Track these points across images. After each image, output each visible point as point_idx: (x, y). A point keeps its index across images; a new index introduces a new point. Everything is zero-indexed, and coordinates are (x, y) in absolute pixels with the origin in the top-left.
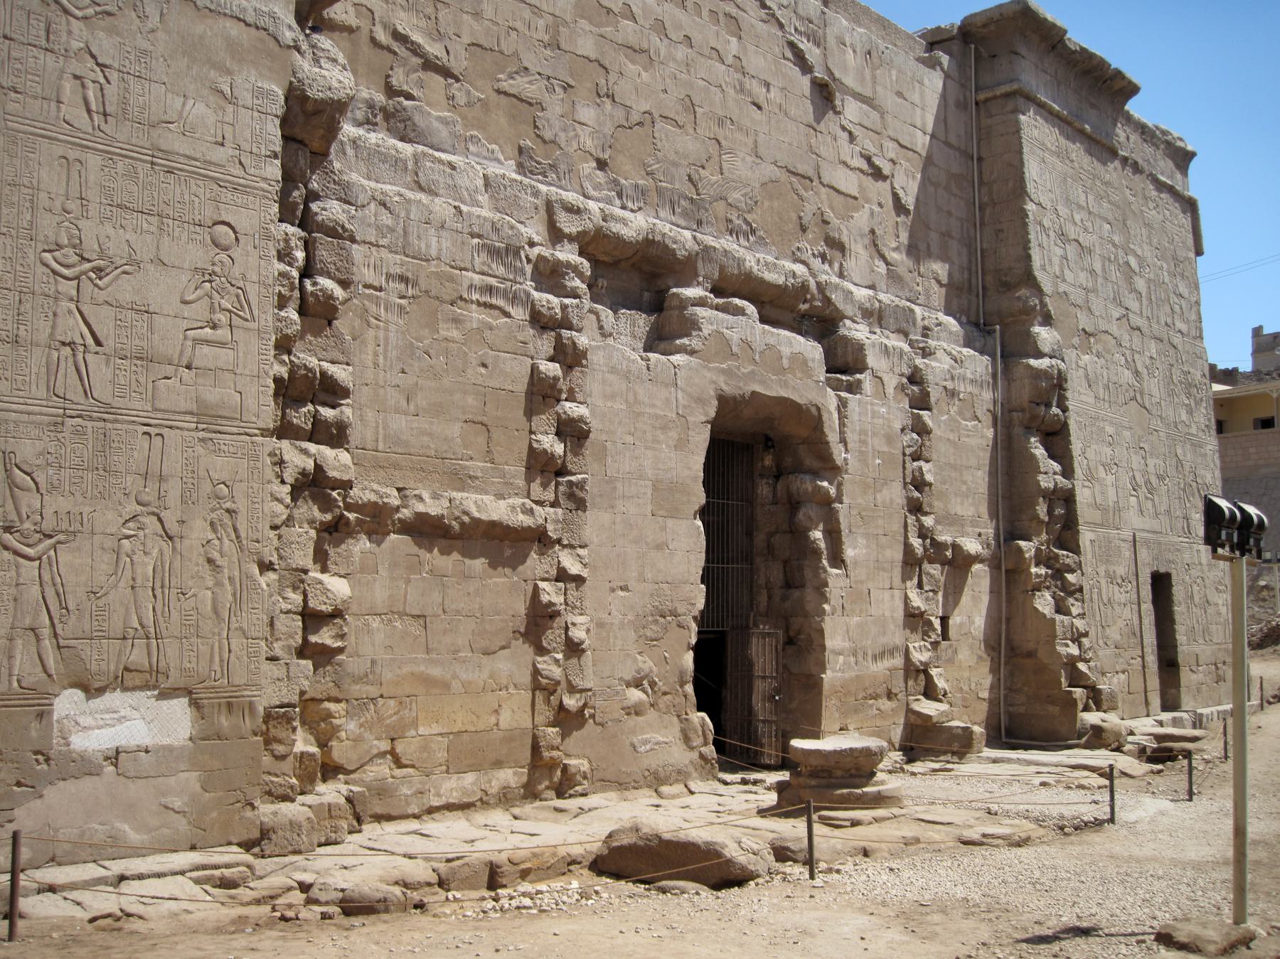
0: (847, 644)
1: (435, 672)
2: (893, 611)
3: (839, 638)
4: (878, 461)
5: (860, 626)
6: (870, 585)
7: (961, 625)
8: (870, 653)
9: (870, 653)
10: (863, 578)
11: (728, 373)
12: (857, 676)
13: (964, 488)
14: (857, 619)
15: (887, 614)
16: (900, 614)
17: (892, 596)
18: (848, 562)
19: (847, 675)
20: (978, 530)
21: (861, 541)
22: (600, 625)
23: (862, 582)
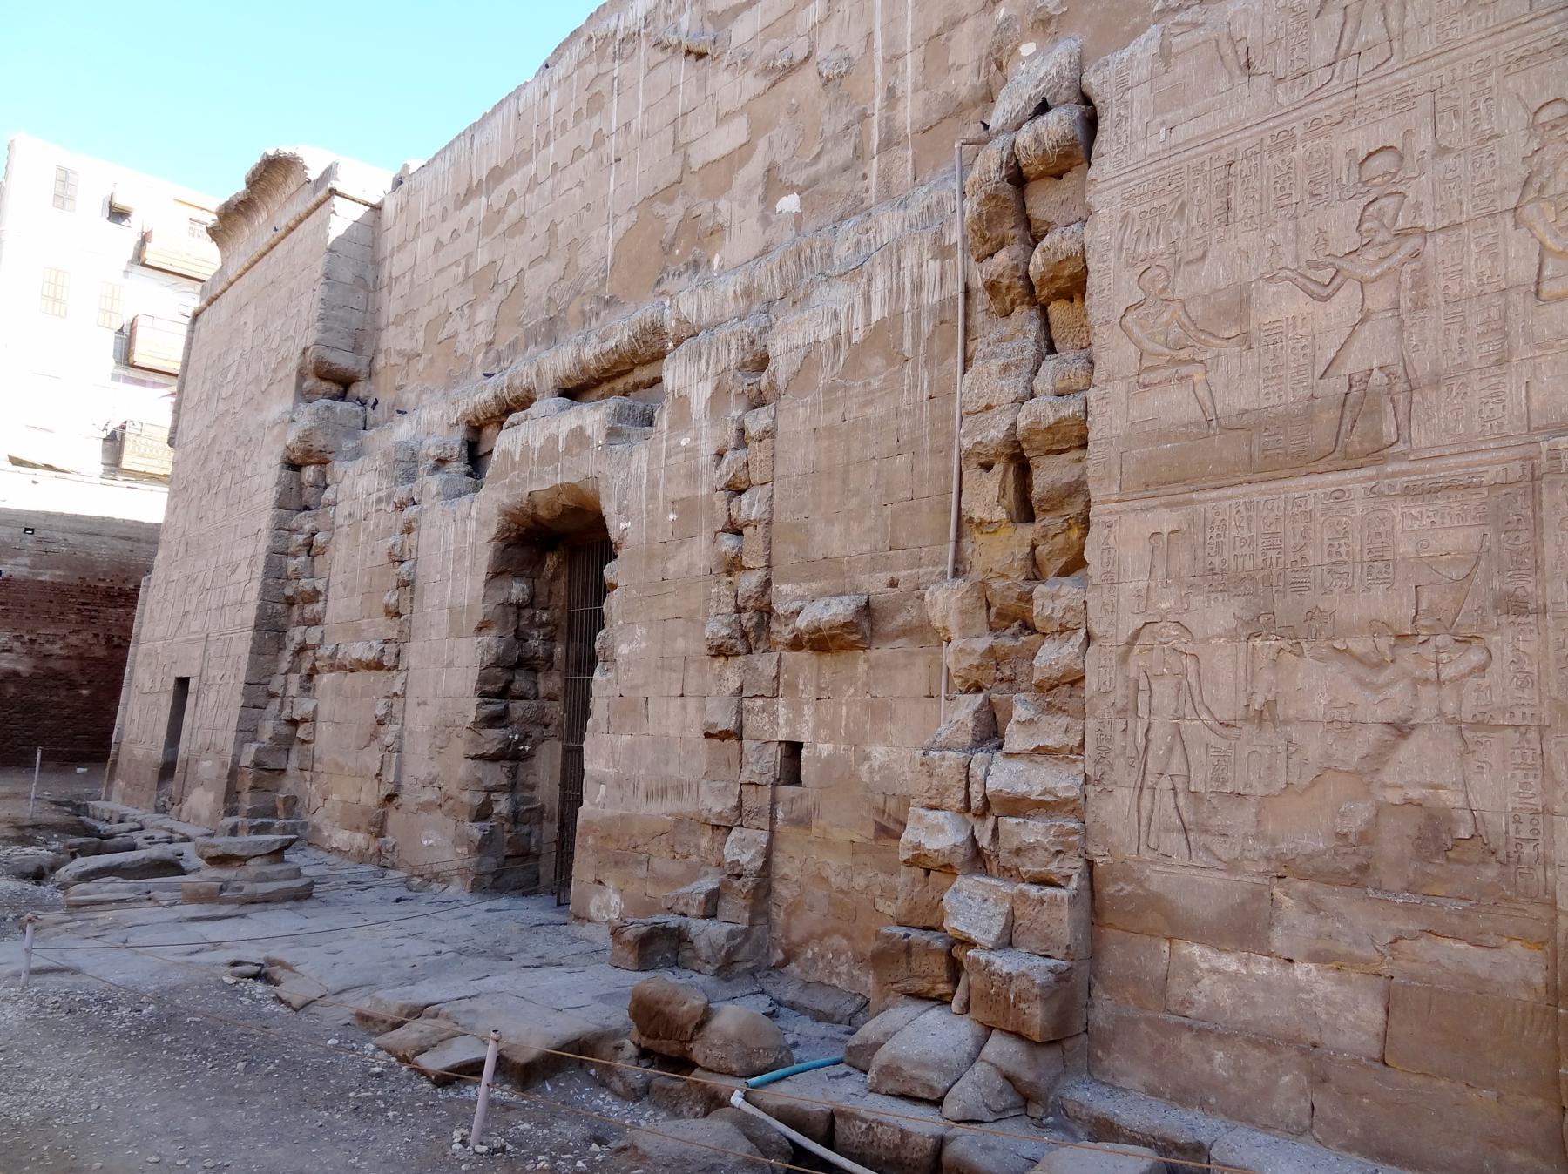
0: (611, 771)
1: (340, 759)
2: (683, 729)
3: (602, 762)
4: (672, 517)
5: (631, 749)
6: (651, 692)
7: (829, 763)
8: (642, 786)
9: (642, 786)
10: (640, 681)
11: (512, 485)
12: (622, 817)
13: (854, 502)
14: (626, 738)
15: (672, 733)
16: (696, 733)
17: (684, 707)
18: (620, 660)
19: (608, 812)
20: (889, 575)
21: (640, 631)
22: (411, 733)
23: (635, 687)
